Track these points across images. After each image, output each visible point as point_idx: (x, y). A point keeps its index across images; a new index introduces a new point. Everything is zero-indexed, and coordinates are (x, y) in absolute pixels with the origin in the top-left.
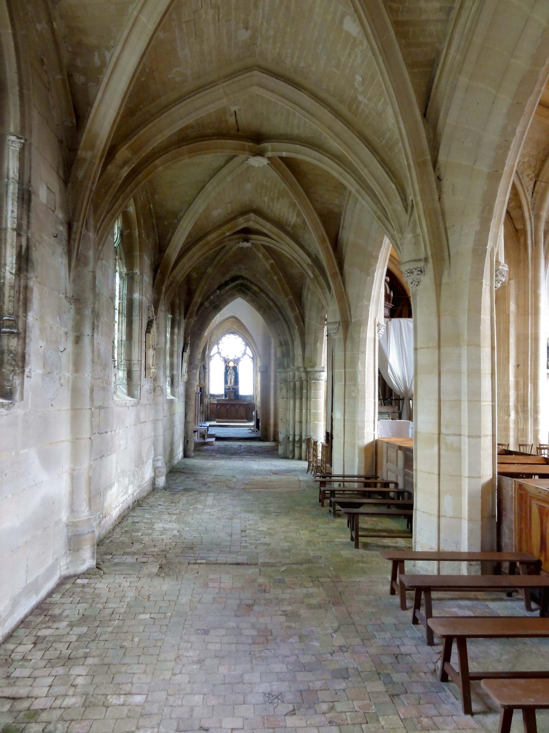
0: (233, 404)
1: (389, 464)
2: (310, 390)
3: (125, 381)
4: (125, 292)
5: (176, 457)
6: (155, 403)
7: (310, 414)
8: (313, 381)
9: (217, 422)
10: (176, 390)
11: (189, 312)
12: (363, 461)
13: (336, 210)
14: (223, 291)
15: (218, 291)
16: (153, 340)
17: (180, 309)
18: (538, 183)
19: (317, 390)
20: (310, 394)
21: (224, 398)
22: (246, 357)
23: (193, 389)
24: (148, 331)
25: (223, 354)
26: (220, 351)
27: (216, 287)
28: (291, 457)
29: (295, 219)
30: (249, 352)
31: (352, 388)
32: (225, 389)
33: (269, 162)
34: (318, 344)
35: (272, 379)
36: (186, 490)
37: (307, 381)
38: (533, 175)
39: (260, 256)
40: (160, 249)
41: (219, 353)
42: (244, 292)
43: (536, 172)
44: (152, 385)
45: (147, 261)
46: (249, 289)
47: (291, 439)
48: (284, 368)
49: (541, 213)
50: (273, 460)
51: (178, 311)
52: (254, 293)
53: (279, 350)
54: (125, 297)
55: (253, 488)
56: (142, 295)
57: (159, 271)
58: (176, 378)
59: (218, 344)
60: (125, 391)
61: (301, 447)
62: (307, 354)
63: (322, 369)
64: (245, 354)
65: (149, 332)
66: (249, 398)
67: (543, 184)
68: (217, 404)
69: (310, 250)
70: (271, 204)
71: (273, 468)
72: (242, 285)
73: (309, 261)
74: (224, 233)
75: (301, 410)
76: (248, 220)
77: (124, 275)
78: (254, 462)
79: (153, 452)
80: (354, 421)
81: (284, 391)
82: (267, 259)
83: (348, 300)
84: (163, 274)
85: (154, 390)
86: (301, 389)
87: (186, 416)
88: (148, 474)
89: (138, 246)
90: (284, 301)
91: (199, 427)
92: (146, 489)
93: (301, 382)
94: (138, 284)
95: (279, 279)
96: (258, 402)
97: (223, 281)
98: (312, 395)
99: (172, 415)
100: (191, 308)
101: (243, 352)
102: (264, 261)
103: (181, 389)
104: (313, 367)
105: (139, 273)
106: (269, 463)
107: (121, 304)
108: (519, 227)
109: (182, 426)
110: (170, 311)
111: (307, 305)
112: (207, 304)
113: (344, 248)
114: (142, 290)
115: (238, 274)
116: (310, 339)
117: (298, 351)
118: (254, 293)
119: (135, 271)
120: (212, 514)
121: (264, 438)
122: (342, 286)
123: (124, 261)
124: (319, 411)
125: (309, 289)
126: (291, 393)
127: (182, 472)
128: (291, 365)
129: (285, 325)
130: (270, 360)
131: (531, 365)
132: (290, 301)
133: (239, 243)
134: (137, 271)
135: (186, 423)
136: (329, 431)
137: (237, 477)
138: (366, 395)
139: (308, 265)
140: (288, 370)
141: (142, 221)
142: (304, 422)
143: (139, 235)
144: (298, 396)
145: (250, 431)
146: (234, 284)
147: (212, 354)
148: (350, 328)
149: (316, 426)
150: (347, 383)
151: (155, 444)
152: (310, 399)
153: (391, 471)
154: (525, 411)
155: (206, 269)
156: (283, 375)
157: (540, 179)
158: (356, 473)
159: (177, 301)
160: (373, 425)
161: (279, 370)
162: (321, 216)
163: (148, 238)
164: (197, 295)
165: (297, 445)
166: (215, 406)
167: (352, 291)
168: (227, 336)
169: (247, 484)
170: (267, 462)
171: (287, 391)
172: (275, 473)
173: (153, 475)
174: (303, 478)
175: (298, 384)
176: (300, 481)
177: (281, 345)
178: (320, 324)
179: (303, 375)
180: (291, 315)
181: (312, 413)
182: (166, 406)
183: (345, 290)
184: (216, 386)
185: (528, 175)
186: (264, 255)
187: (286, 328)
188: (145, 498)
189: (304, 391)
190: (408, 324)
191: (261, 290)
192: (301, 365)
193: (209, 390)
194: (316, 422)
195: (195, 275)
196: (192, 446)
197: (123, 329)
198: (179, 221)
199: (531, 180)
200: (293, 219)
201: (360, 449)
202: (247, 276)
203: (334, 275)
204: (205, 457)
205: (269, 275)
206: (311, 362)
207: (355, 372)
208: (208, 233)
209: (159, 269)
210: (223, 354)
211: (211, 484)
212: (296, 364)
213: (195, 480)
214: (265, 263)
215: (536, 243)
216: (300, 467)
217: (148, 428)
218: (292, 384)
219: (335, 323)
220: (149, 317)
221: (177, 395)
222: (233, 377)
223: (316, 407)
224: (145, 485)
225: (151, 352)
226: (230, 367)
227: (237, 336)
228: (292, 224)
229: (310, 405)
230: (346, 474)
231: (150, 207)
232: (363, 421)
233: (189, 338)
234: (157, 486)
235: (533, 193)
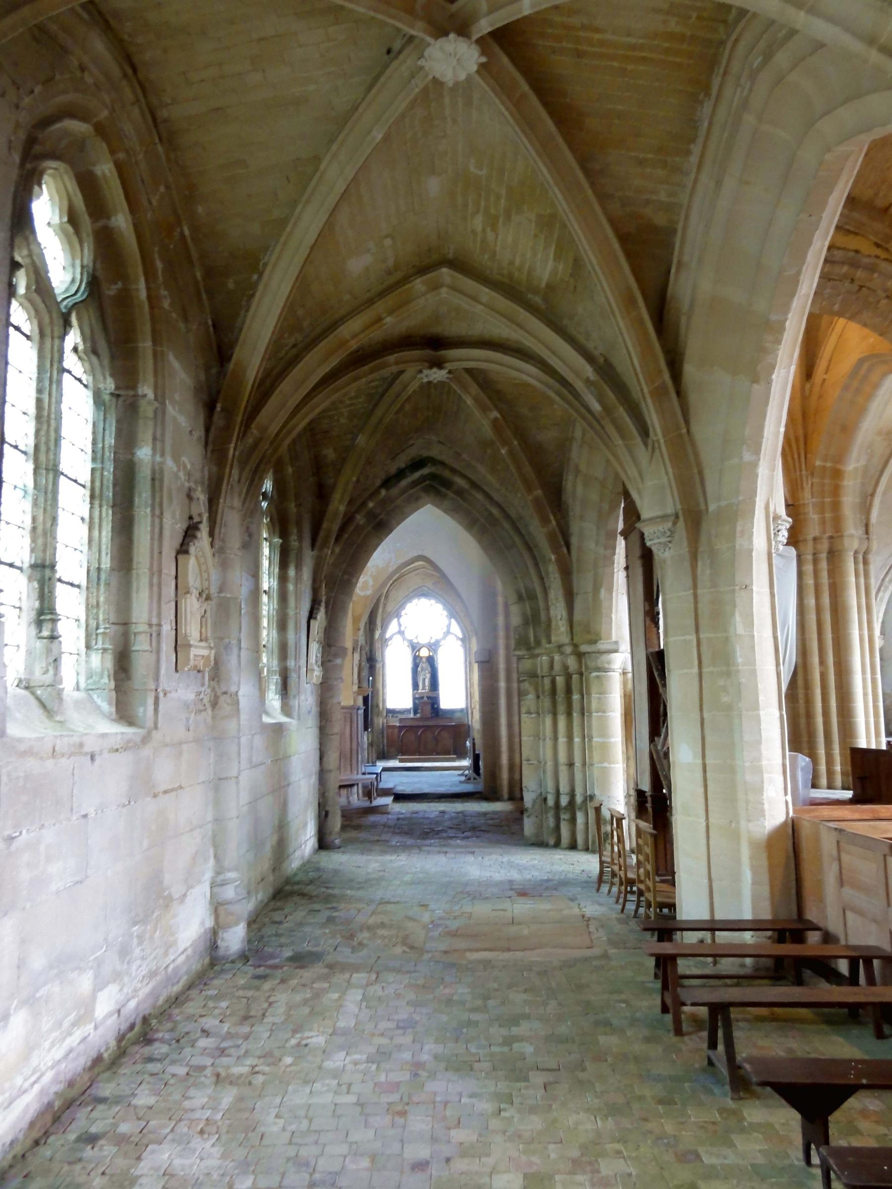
0: (428, 727)
1: (847, 891)
2: (589, 694)
3: (108, 682)
4: (110, 440)
5: (298, 854)
6: (217, 737)
7: (590, 747)
8: (594, 674)
9: (401, 761)
10: (294, 703)
11: (322, 534)
12: (765, 878)
13: (660, 220)
14: (395, 491)
15: (383, 492)
16: (205, 575)
17: (299, 524)
19: (603, 692)
20: (590, 702)
21: (412, 716)
22: (450, 638)
23: (335, 700)
24: (183, 550)
25: (409, 635)
27: (378, 482)
28: (552, 842)
29: (550, 264)
31: (721, 683)
32: (414, 699)
33: (484, 59)
34: (603, 592)
35: (502, 676)
36: (300, 960)
37: (581, 674)
39: (469, 401)
40: (219, 349)
41: (401, 633)
42: (438, 493)
44: (206, 689)
45: (181, 376)
46: (447, 484)
47: (551, 802)
48: (529, 648)
50: (514, 850)
51: (295, 531)
52: (460, 493)
53: (515, 609)
54: (109, 455)
55: (470, 950)
56: (163, 455)
57: (218, 409)
58: (293, 676)
59: (398, 616)
60: (107, 707)
61: (573, 820)
62: (577, 617)
63: (613, 647)
64: (448, 632)
65: (186, 552)
66: (458, 715)
68: (401, 728)
69: (590, 345)
70: (490, 236)
71: (515, 875)
72: (433, 477)
73: (589, 371)
74: (380, 319)
75: (570, 738)
76: (435, 287)
77: (107, 398)
78: (471, 858)
79: (212, 862)
80: (730, 770)
81: (531, 696)
82: (484, 409)
83: (697, 455)
84: (229, 413)
85: (214, 704)
86: (569, 691)
87: (321, 758)
88: (190, 924)
89: (148, 328)
90: (522, 502)
91: (360, 776)
92: (184, 969)
93: (568, 677)
94: (151, 424)
95: (511, 452)
96: (475, 721)
97: (393, 469)
98: (594, 705)
99: (278, 761)
100: (325, 525)
101: (445, 630)
102: (477, 413)
103: (306, 699)
104: (595, 642)
105: (151, 395)
106: (505, 859)
107: (98, 474)
109: (314, 779)
110: (277, 529)
111: (575, 510)
112: (360, 519)
113: (683, 320)
114: (163, 441)
115: (425, 453)
116: (583, 583)
117: (558, 611)
118: (460, 493)
119: (140, 392)
120: (346, 1078)
121: (490, 794)
122: (682, 421)
123: (106, 362)
124: (612, 740)
125: (578, 471)
126: (547, 702)
127: (303, 895)
128: (544, 641)
129: (527, 556)
130: (496, 637)
132: (537, 502)
133: (420, 372)
134: (146, 390)
135: (322, 774)
136: (646, 786)
137: (432, 906)
138: (761, 698)
139: (588, 382)
140: (537, 651)
141: (159, 265)
142: (578, 764)
143: (149, 297)
144: (561, 708)
145: (463, 778)
146: (417, 475)
147: (388, 635)
148: (704, 526)
149: (606, 774)
150: (704, 670)
151: (217, 843)
152: (590, 713)
153: (860, 912)
155: (354, 439)
156: (527, 664)
158: (748, 915)
159: (292, 507)
161: (518, 653)
162: (623, 239)
163: (186, 319)
164: (337, 496)
165: (565, 816)
166: (396, 731)
167: (707, 431)
168: (415, 601)
169: (454, 934)
170: (500, 858)
171: (538, 697)
172: (523, 892)
173: (209, 923)
174: (591, 909)
175: (560, 681)
176: (586, 920)
177: (520, 598)
178: (606, 548)
179: (572, 662)
180: (539, 532)
181: (594, 744)
182: (259, 742)
183: (688, 431)
184: (398, 694)
186: (476, 399)
187: (530, 564)
188: (177, 1001)
189: (576, 697)
191: (474, 485)
192: (565, 639)
193: (384, 701)
194: (606, 765)
195: (330, 453)
196: (336, 822)
197: (104, 540)
198: (261, 275)
200: (543, 266)
201: (754, 845)
202: (443, 458)
203: (659, 394)
204: (367, 846)
205: (489, 451)
206: (589, 632)
207: (727, 639)
208: (342, 320)
209: (223, 409)
210: (409, 635)
211: (364, 936)
212: (553, 639)
213: (330, 920)
214: (480, 421)
216: (578, 869)
217: (190, 808)
218: (547, 681)
219: (664, 517)
220: (191, 518)
221: (295, 714)
222: (428, 676)
223: (605, 732)
224: (183, 957)
225: (192, 605)
226: (421, 658)
227: (433, 601)
228: (543, 285)
229: (590, 727)
230: (718, 917)
231: (182, 234)
232: (759, 771)
233: (323, 591)
234: (221, 952)
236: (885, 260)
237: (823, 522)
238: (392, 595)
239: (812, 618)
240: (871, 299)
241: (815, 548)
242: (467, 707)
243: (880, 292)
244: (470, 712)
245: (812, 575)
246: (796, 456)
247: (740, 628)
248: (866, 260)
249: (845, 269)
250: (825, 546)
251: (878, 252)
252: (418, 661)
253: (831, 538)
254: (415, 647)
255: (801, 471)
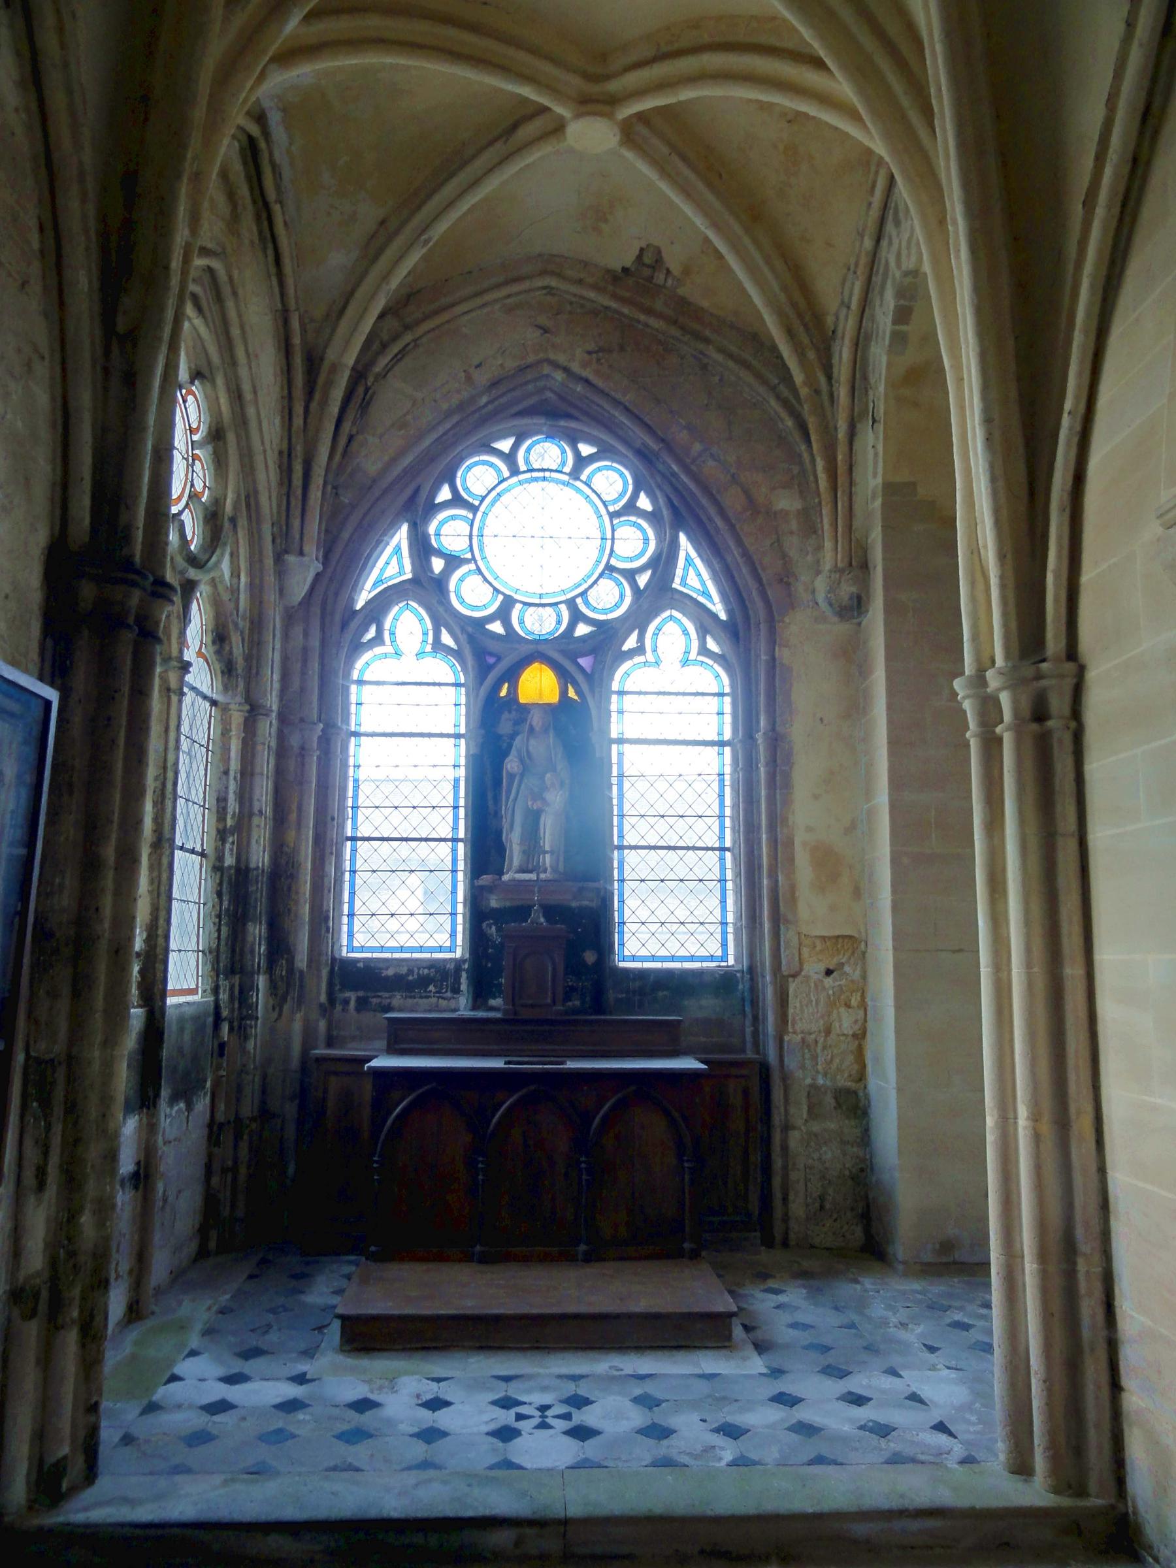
25: (471, 595)
26: (438, 564)
30: (695, 574)
32: (479, 915)
41: (428, 588)
59: (419, 510)
64: (656, 593)
66: (705, 1006)
166: (367, 1090)
193: (323, 923)
210: (471, 595)
226: (525, 709)
238: (395, 396)
242: (751, 969)
244: (769, 994)
252: (505, 728)
254: (488, 656)
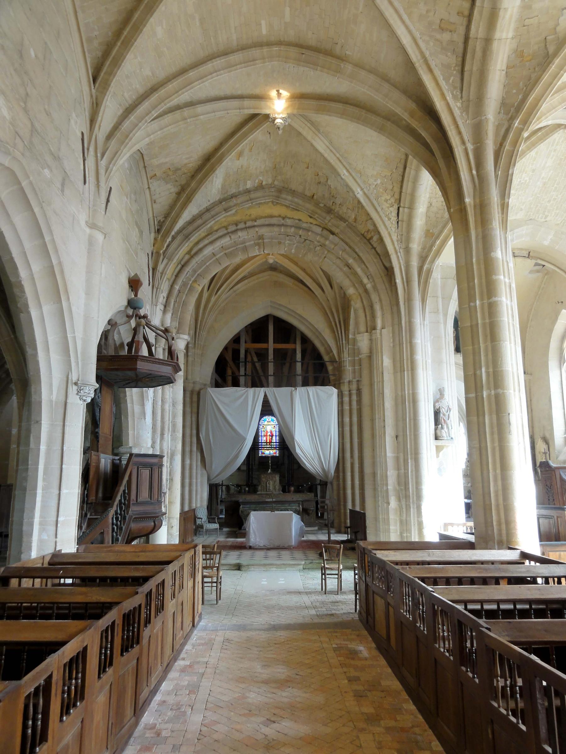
18: (401, 209)
38: (393, 200)
43: (397, 196)
49: (411, 245)
67: (406, 210)
108: (387, 265)
131: (410, 435)
154: (407, 497)
157: (402, 205)
160: (54, 528)
183: (16, 337)
185: (386, 201)
190: (316, 391)
199: (392, 206)
215: (408, 282)
235: (398, 222)
236: (316, 225)
237: (354, 372)
239: (347, 429)
240: (311, 247)
241: (349, 387)
243: (316, 243)
245: (348, 405)
246: (339, 332)
247: (32, 445)
248: (304, 225)
249: (293, 230)
250: (354, 386)
251: (311, 220)
253: (358, 381)
255: (342, 341)
